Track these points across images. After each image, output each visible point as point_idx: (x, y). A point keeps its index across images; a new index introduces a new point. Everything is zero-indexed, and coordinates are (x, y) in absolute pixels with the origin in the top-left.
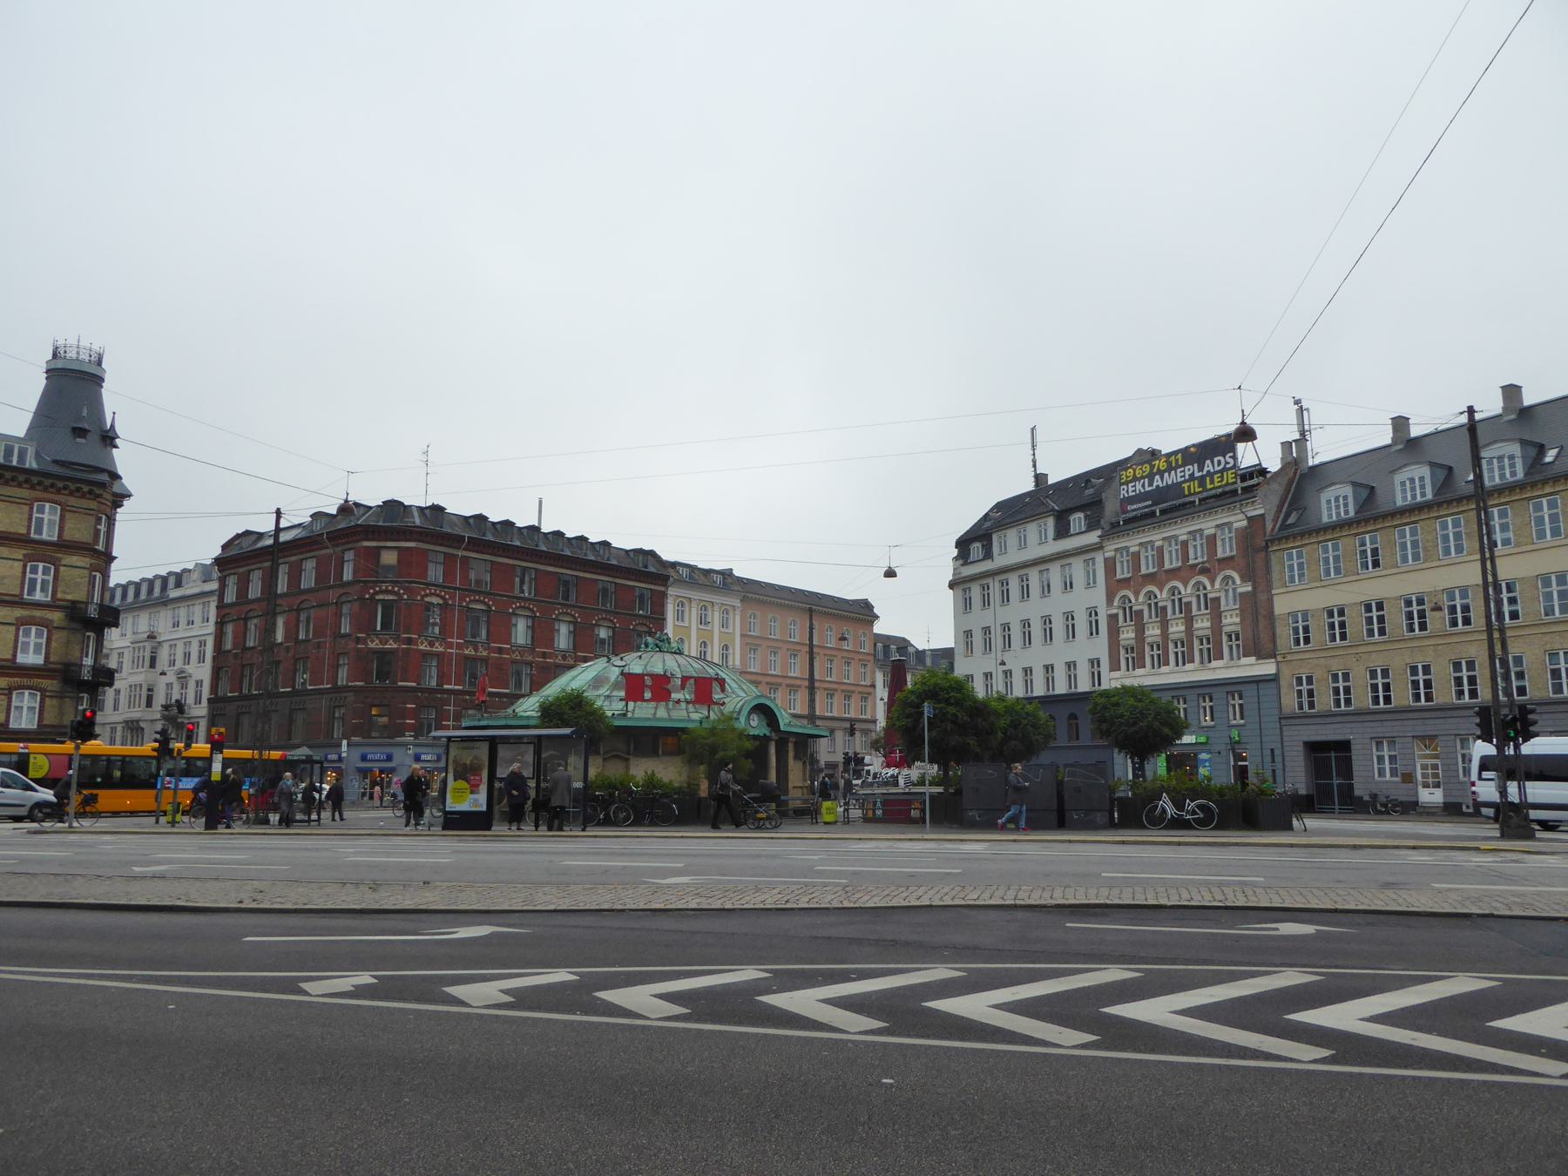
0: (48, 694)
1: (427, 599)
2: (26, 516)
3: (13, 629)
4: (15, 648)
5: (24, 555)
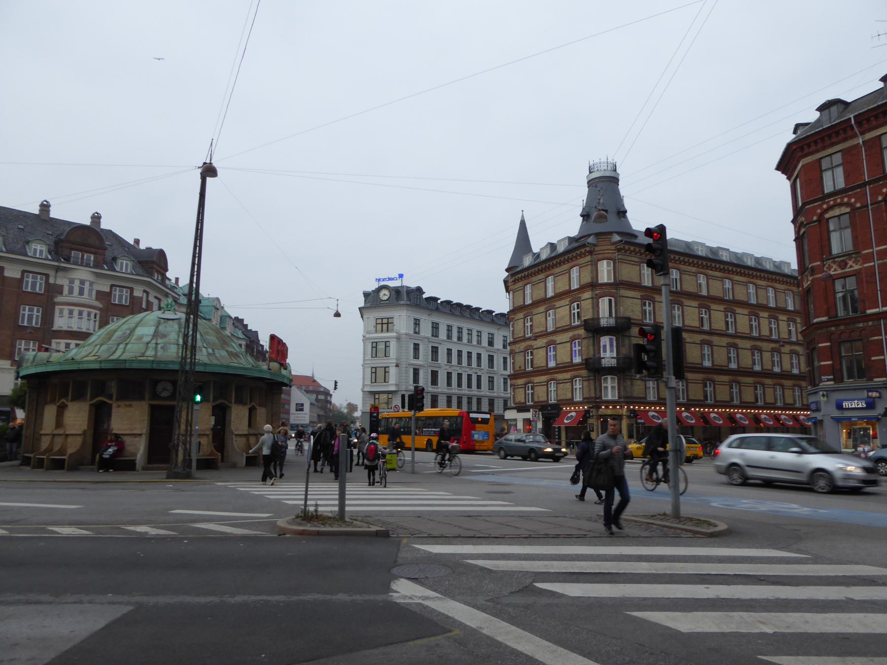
0: (584, 379)
1: (827, 216)
2: (568, 279)
3: (569, 344)
4: (571, 355)
5: (569, 301)
